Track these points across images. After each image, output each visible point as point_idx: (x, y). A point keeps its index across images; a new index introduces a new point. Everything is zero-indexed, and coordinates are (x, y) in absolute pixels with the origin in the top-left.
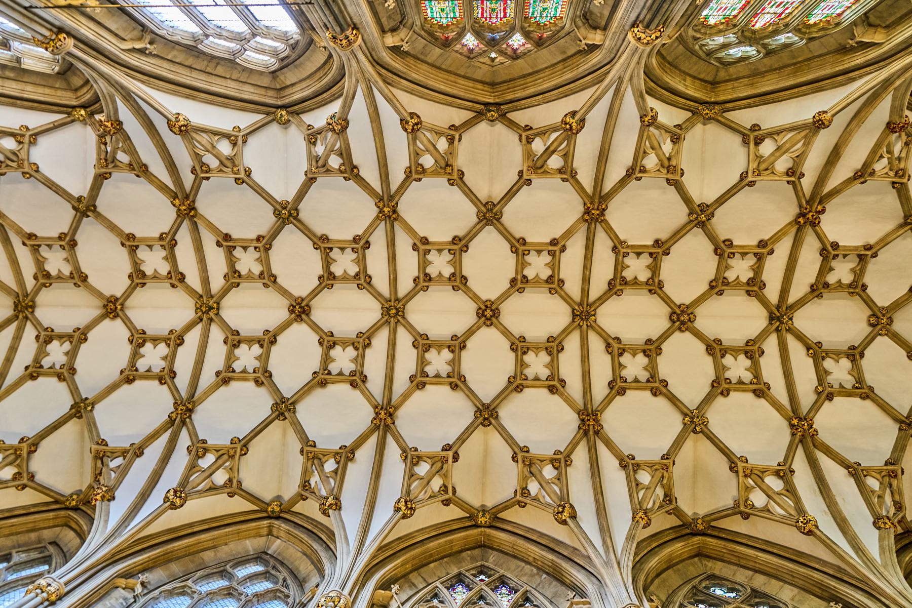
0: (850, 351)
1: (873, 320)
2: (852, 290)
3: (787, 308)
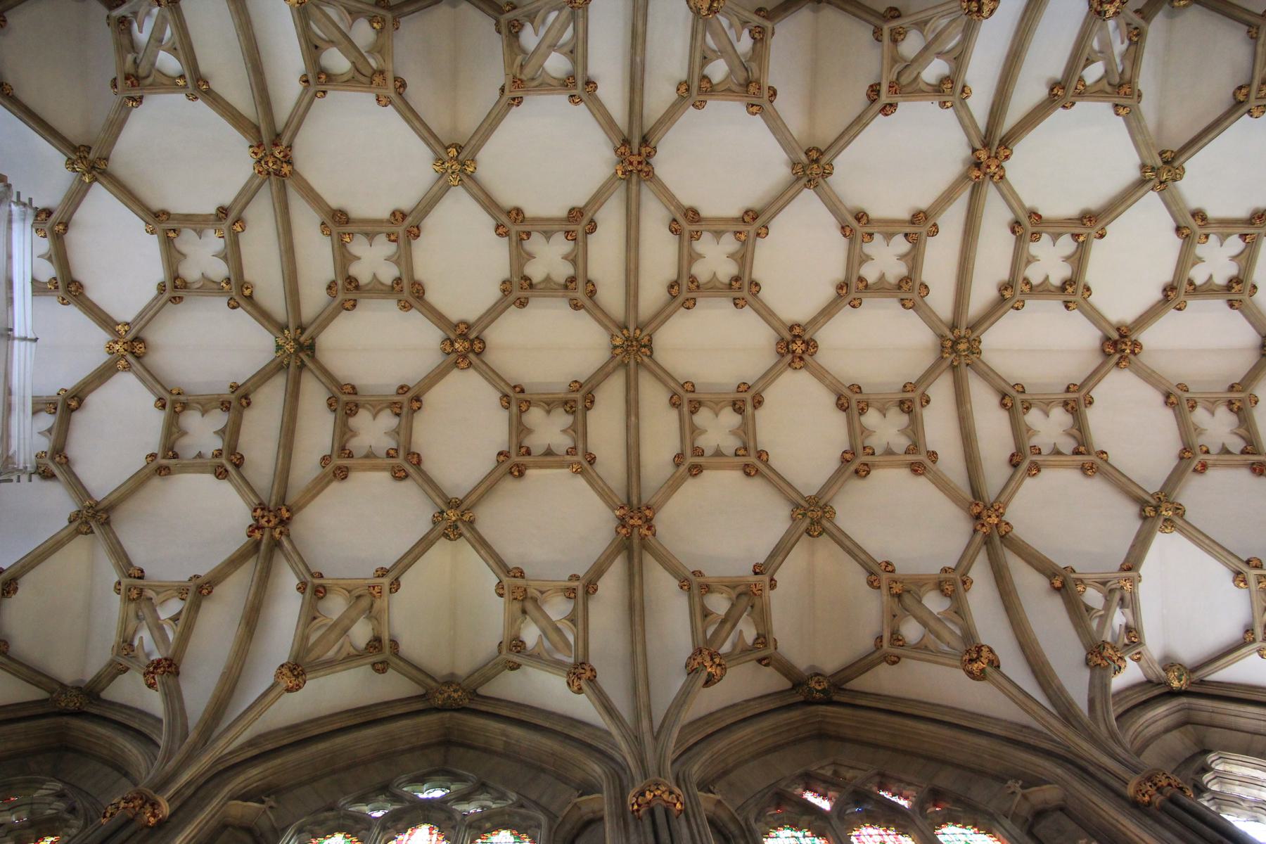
1: (139, 348)
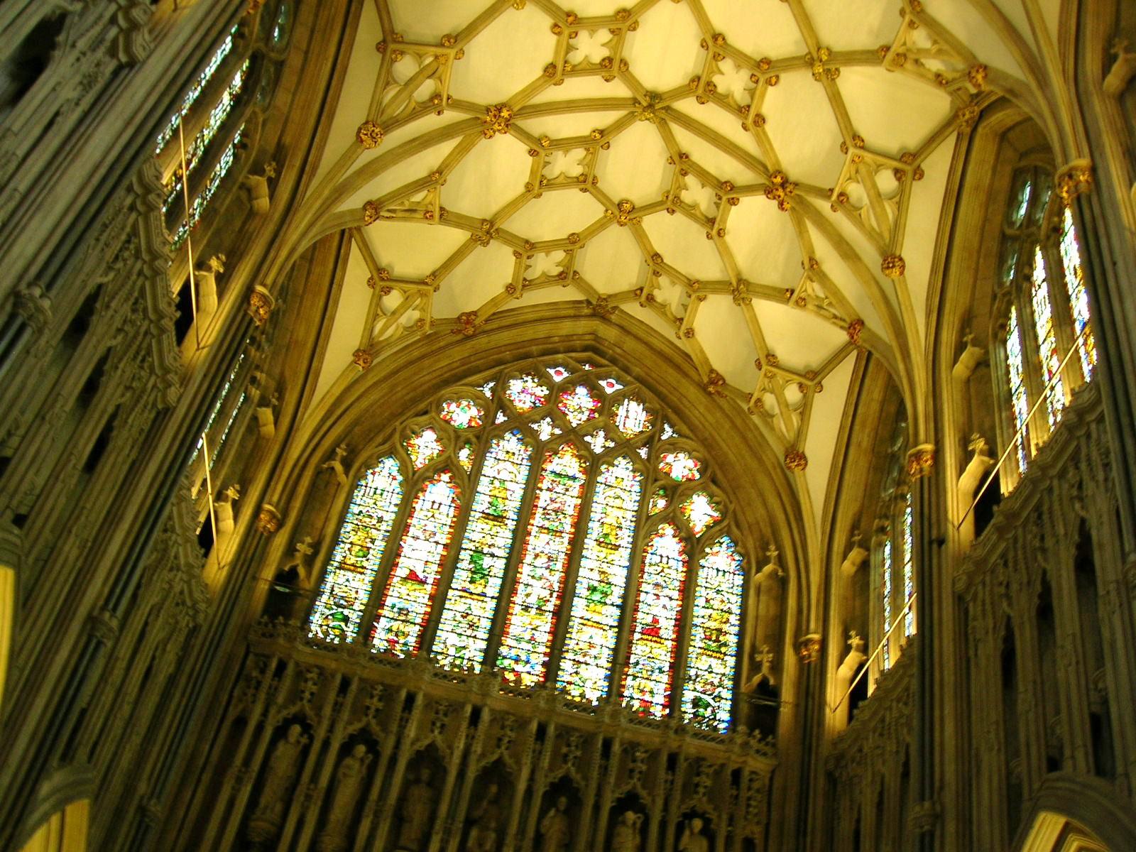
0: (590, 180)
1: (627, 207)
2: (671, 198)
3: (663, 119)
